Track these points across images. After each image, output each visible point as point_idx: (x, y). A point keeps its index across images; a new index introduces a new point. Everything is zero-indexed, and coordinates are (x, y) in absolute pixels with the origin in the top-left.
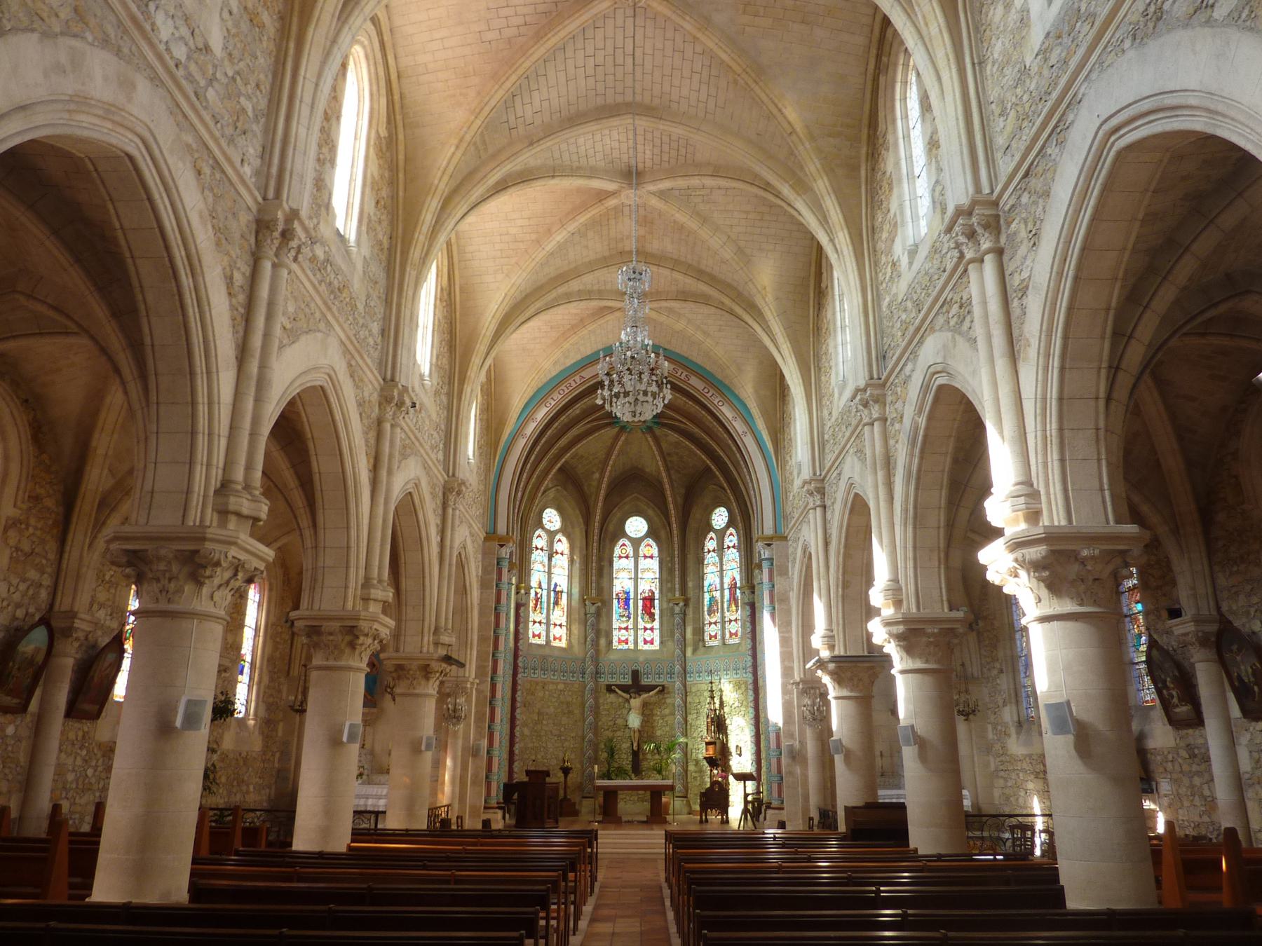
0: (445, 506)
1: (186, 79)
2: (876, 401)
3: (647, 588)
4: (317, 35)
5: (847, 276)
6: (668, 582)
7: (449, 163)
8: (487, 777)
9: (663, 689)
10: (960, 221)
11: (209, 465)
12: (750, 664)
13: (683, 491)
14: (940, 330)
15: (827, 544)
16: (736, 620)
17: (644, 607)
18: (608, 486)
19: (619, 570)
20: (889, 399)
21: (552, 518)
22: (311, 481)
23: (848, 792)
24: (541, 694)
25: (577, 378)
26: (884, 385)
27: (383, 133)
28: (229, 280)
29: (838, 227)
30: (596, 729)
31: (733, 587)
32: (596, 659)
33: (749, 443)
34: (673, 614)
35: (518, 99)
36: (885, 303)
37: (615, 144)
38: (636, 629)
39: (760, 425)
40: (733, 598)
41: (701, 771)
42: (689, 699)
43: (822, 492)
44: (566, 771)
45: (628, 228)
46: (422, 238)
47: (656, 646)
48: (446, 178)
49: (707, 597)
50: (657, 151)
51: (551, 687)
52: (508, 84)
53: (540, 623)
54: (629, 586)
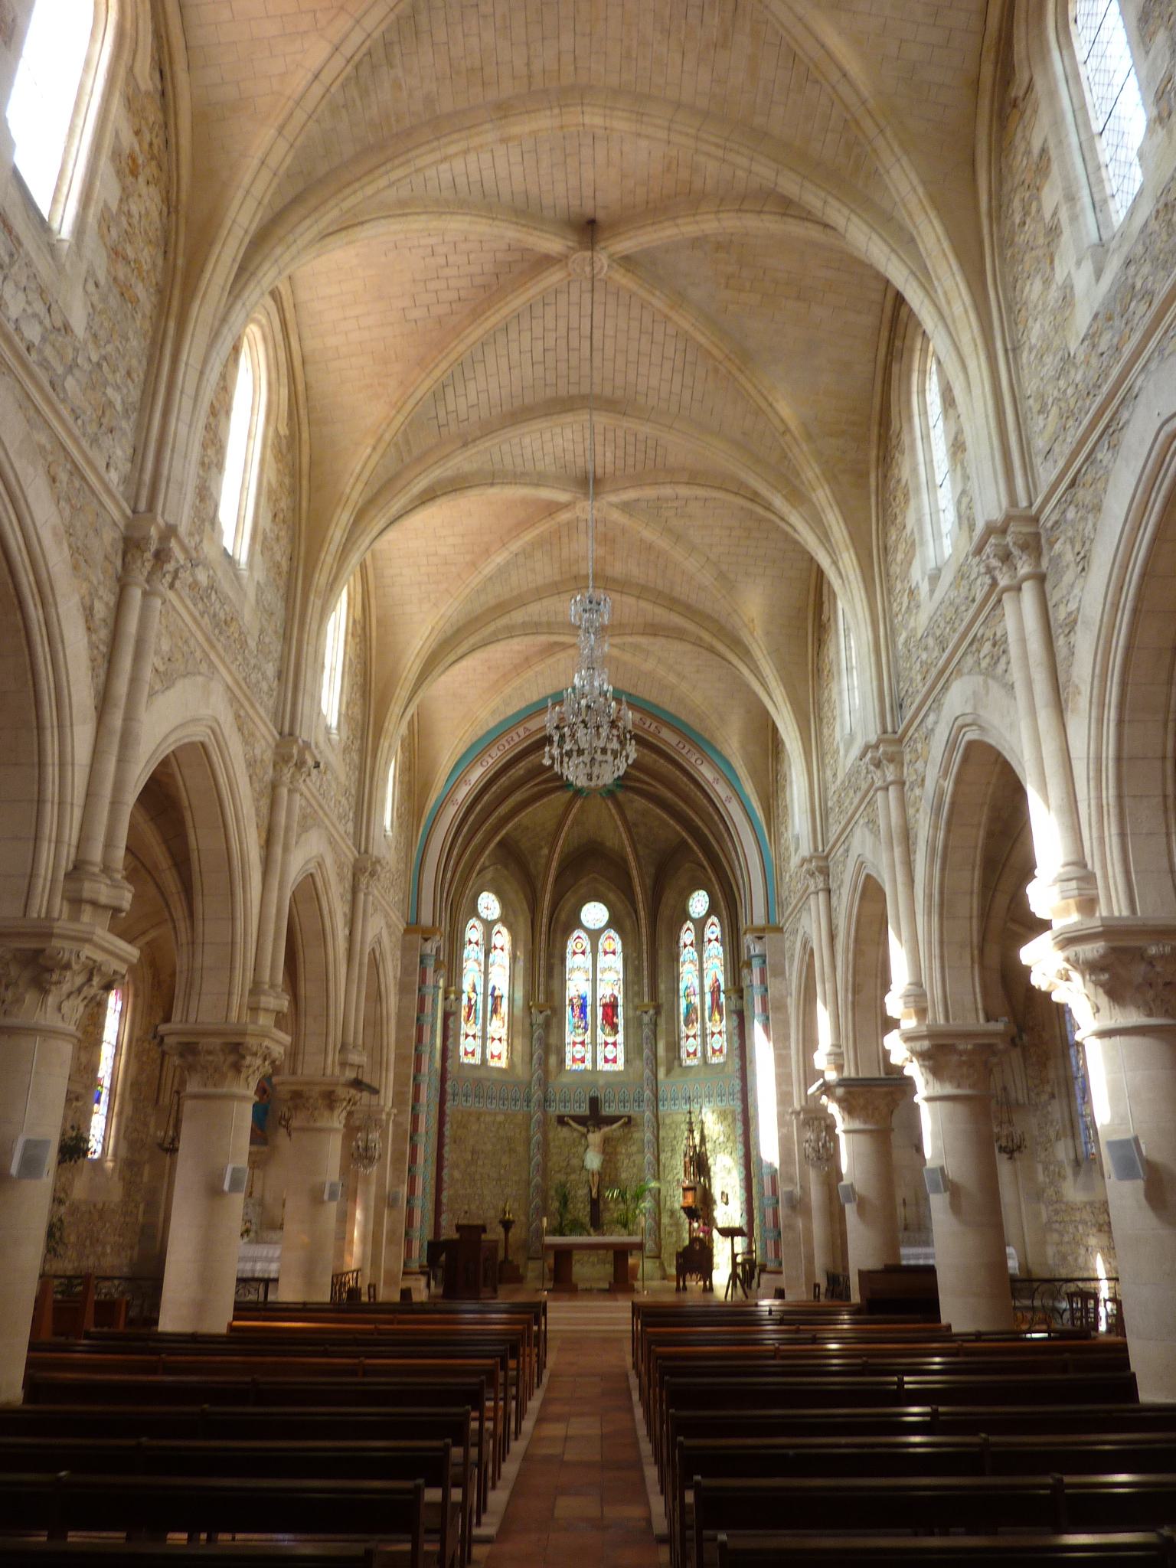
0: (355, 890)
1: (40, 365)
2: (891, 760)
3: (608, 993)
4: (203, 313)
5: (854, 607)
6: (634, 983)
7: (363, 467)
8: (407, 1234)
9: (629, 1122)
10: (992, 540)
11: (59, 841)
12: (738, 1088)
13: (652, 870)
14: (970, 673)
15: (832, 937)
17: (605, 1016)
18: (560, 865)
19: (572, 970)
20: (907, 758)
21: (489, 904)
22: (187, 860)
23: (863, 1251)
24: (475, 1127)
25: (521, 731)
26: (900, 740)
27: (284, 430)
28: (89, 612)
29: (842, 546)
30: (544, 1170)
31: (716, 991)
32: (544, 1083)
33: (734, 809)
34: (640, 1024)
35: (450, 390)
36: (901, 640)
37: (569, 446)
39: (749, 789)
40: (716, 1005)
41: (677, 1225)
42: (662, 1133)
43: (825, 872)
44: (507, 1225)
45: (584, 549)
46: (329, 559)
47: (620, 1066)
48: (360, 486)
49: (683, 1003)
50: (620, 453)
51: (488, 1119)
52: (437, 373)
54: (585, 989)
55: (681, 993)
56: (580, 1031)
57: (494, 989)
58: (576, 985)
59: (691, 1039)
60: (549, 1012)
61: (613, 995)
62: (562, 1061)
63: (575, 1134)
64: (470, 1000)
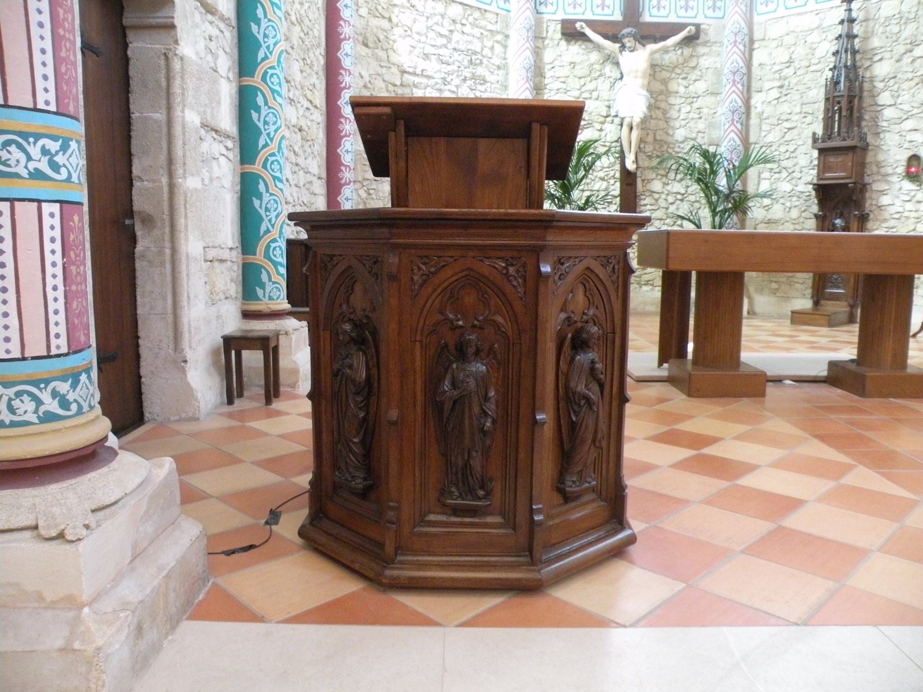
63: (595, 56)
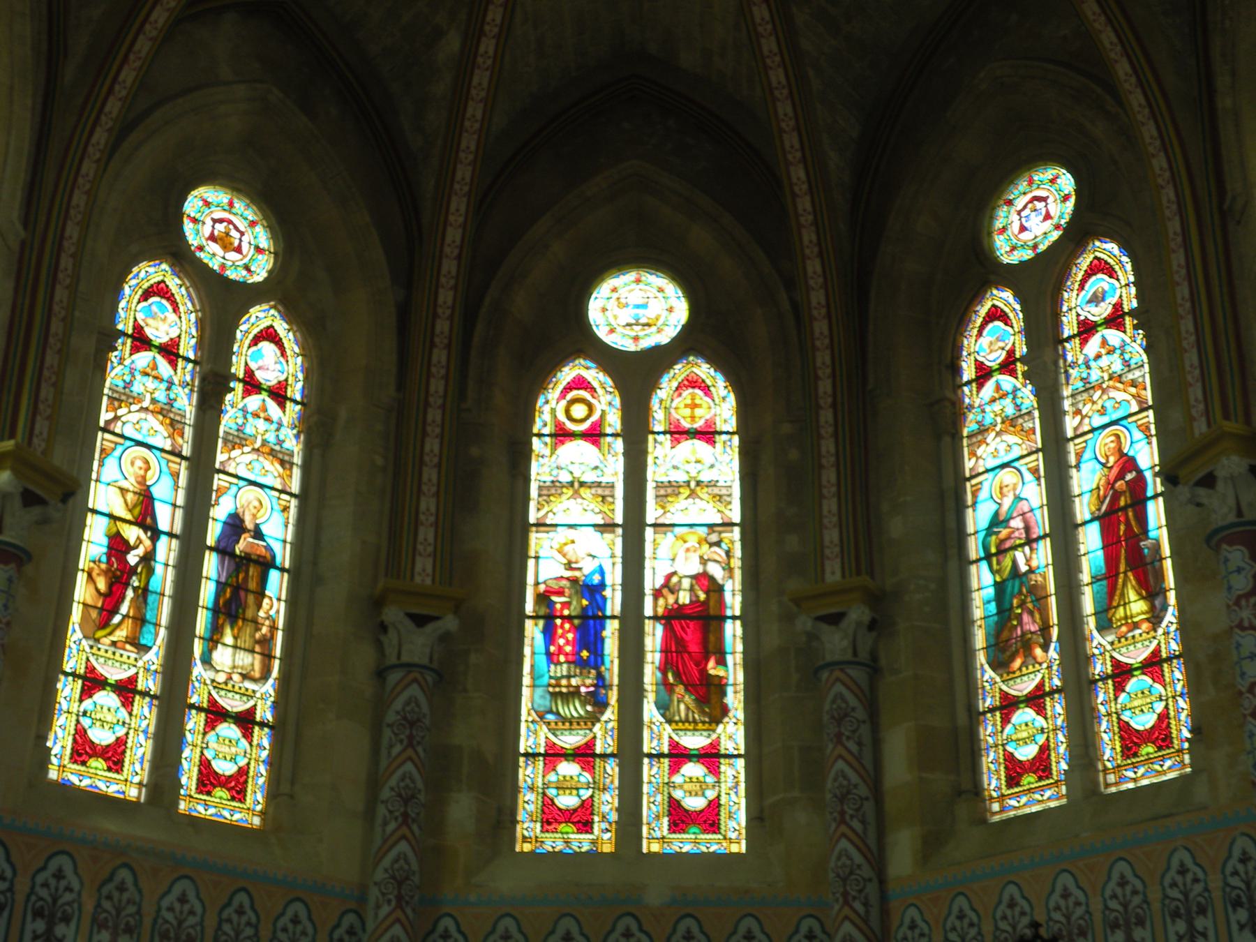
16: (1153, 665)
19: (552, 489)
21: (227, 227)
38: (630, 753)
47: (733, 836)
49: (982, 580)
53: (127, 690)
54: (600, 556)
55: (974, 548)
56: (575, 709)
57: (235, 525)
58: (567, 542)
59: (1024, 715)
60: (450, 623)
61: (703, 579)
62: (502, 819)
64: (118, 546)
